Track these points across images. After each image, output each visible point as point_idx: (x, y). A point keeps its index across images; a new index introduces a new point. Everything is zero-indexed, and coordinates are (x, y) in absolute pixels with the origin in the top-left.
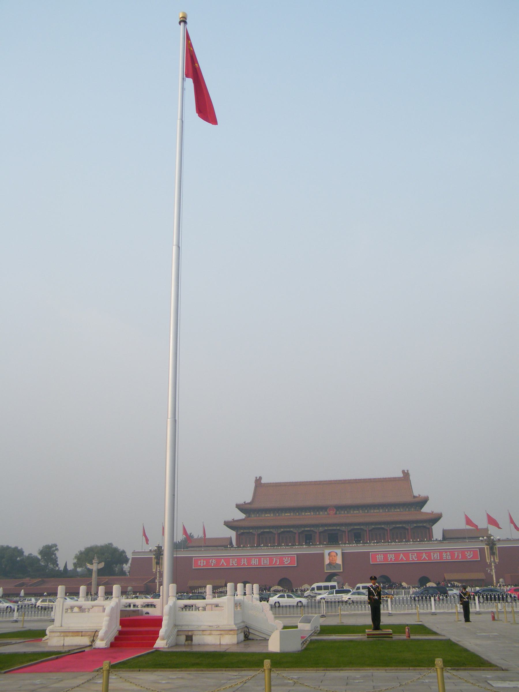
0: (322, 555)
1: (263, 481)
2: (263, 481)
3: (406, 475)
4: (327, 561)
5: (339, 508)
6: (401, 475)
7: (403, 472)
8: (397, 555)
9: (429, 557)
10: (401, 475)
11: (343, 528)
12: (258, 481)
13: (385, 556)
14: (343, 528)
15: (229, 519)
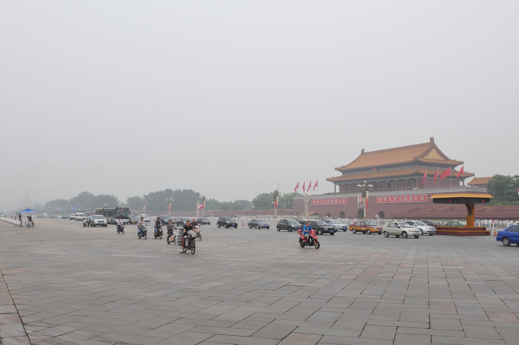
0: (357, 197)
1: (365, 152)
2: (365, 152)
3: (432, 140)
4: (359, 202)
5: (379, 168)
6: (429, 141)
7: (431, 138)
8: (388, 198)
9: (402, 199)
10: (429, 141)
11: (376, 181)
12: (363, 151)
13: (383, 198)
14: (376, 181)
15: (330, 177)
